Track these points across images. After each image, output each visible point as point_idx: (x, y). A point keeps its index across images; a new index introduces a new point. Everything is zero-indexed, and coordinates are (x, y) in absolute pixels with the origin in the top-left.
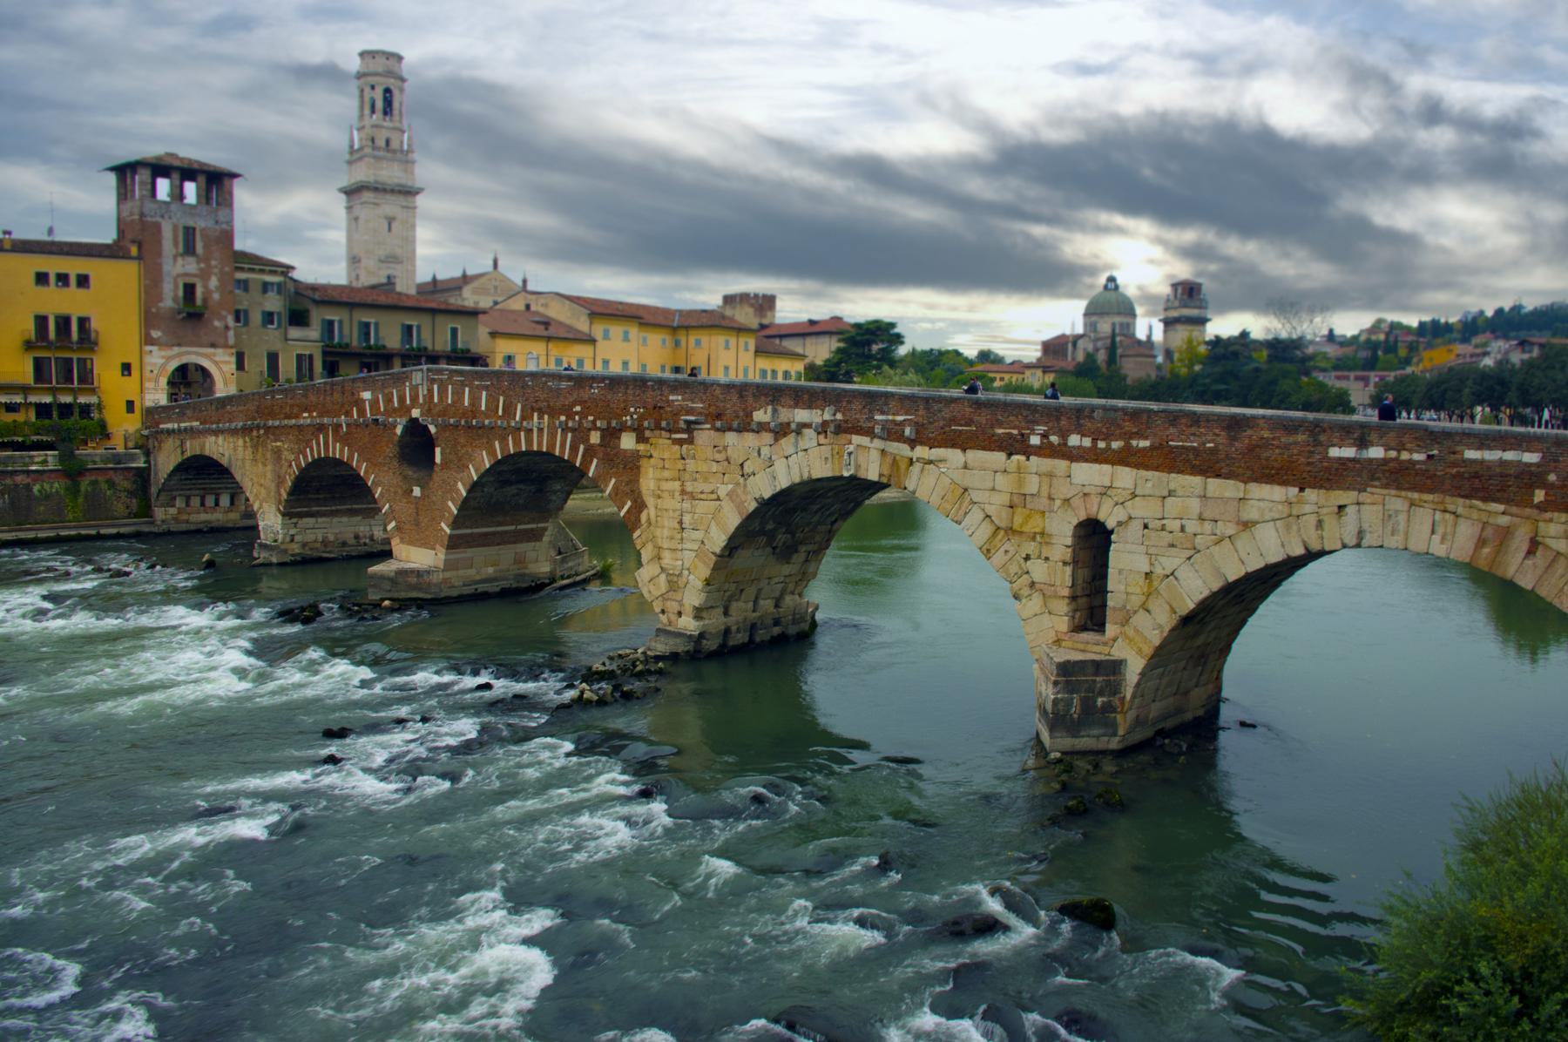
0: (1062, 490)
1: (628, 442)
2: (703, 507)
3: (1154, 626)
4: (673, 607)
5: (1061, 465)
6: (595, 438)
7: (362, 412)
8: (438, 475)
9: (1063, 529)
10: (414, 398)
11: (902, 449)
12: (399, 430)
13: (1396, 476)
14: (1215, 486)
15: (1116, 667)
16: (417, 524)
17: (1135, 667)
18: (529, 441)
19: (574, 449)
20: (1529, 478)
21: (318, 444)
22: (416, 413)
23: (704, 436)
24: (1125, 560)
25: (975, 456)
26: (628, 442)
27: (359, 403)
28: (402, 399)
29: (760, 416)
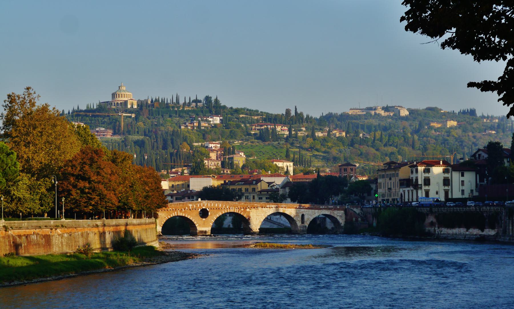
0: (300, 212)
1: (248, 210)
2: (259, 217)
3: (308, 223)
4: (255, 229)
5: (300, 209)
6: (242, 210)
7: (189, 208)
8: (209, 217)
9: (300, 215)
10: (204, 205)
11: (285, 209)
12: (200, 210)
13: (325, 209)
14: (313, 210)
15: (306, 226)
16: (204, 224)
17: (307, 226)
18: (230, 210)
19: (239, 211)
20: (332, 208)
21: (175, 213)
22: (204, 208)
23: (260, 209)
24: (306, 217)
25: (292, 209)
26: (248, 210)
27: (189, 207)
28: (200, 206)
29: (268, 206)
